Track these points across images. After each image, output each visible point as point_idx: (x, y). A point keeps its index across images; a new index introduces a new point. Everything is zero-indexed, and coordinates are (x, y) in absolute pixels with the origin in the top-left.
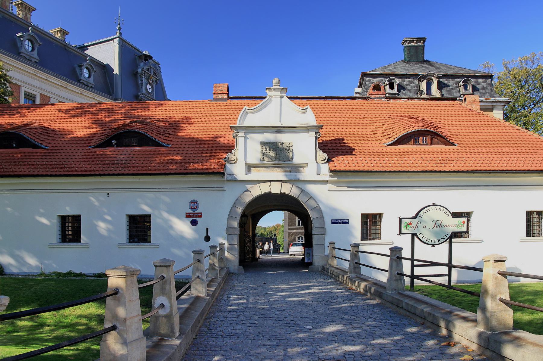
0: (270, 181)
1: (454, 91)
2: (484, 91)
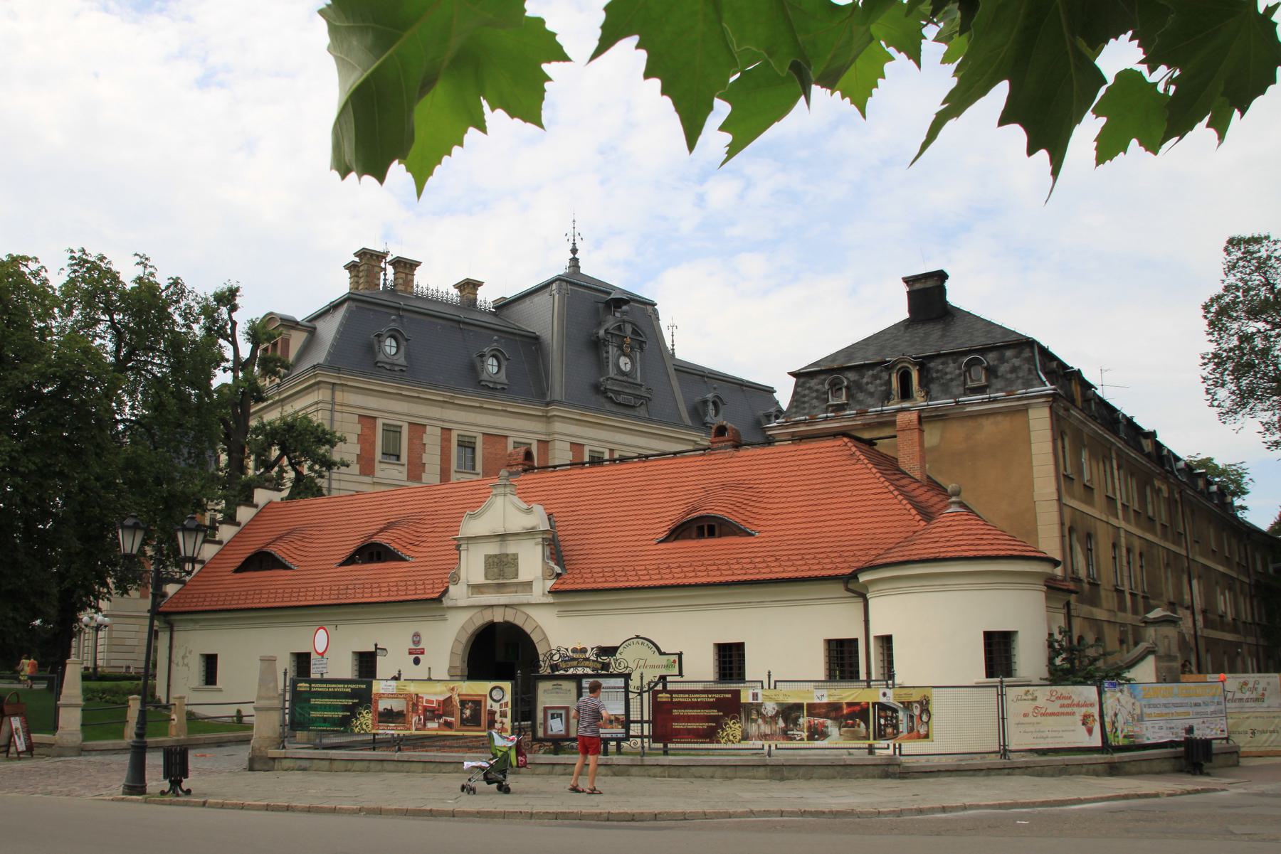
0: (492, 606)
1: (954, 383)
2: (1014, 375)
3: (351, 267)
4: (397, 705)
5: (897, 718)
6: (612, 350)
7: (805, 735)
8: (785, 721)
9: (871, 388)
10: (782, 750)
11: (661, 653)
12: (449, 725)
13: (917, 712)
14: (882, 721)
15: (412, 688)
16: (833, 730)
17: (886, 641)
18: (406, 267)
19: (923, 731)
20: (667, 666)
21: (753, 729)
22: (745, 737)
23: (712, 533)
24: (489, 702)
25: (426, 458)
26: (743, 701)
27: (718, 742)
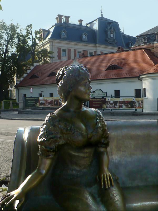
3: (57, 18)
4: (43, 102)
5: (136, 104)
6: (109, 33)
7: (118, 107)
8: (114, 104)
9: (152, 39)
10: (114, 110)
11: (103, 92)
12: (52, 105)
13: (140, 103)
14: (133, 105)
15: (46, 99)
16: (124, 106)
17: (145, 89)
18: (67, 18)
19: (141, 106)
20: (104, 95)
21: (108, 106)
22: (107, 107)
23: (115, 69)
24: (59, 101)
25: (71, 56)
26: (106, 100)
27: (102, 108)
